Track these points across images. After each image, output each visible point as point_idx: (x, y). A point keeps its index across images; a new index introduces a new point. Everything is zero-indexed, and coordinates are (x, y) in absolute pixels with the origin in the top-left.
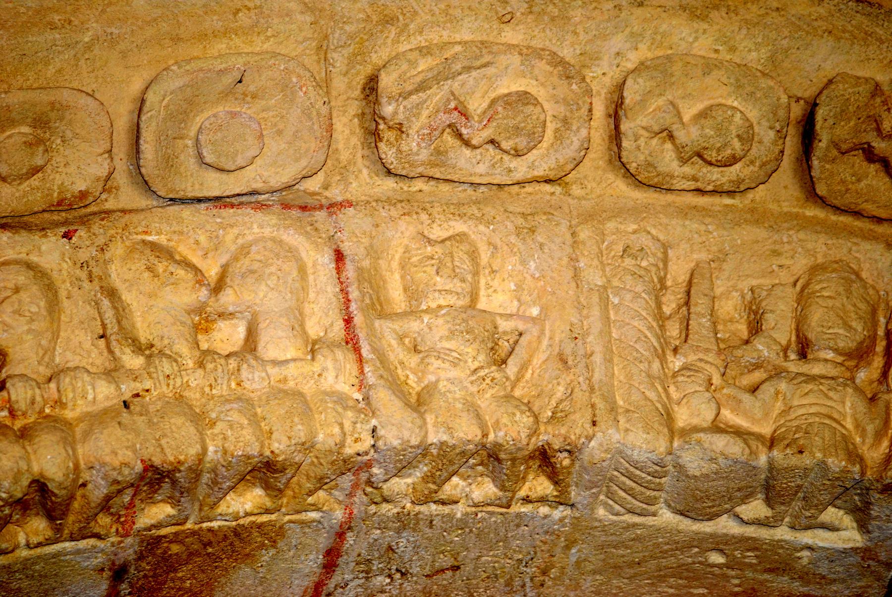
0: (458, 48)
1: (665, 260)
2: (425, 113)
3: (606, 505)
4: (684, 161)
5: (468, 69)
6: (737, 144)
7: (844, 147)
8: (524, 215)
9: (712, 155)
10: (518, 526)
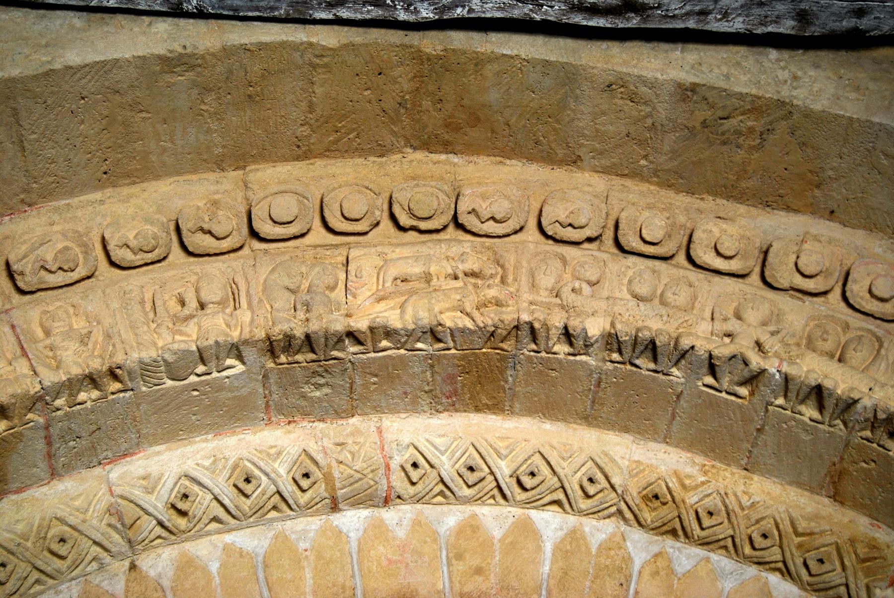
0: (36, 238)
1: (142, 293)
2: (30, 265)
3: (145, 386)
4: (135, 254)
5: (42, 245)
6: (153, 241)
7: (193, 230)
8: (83, 292)
9: (145, 249)
10: (115, 404)
